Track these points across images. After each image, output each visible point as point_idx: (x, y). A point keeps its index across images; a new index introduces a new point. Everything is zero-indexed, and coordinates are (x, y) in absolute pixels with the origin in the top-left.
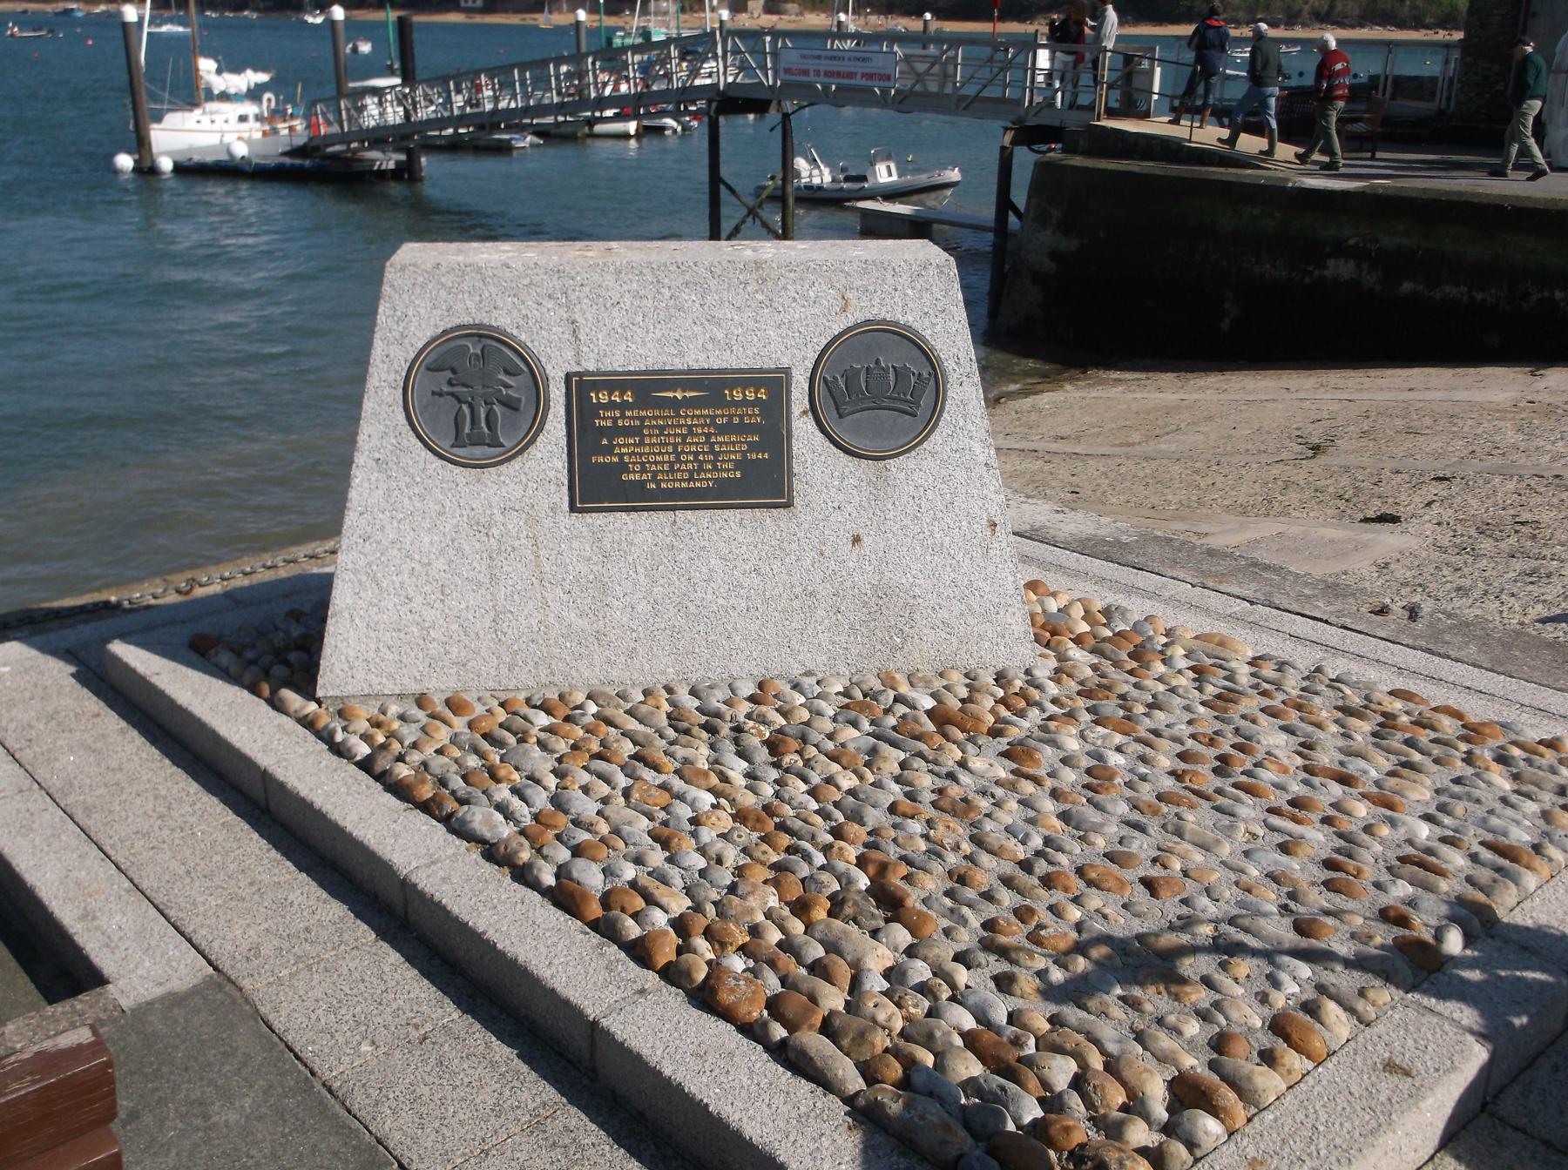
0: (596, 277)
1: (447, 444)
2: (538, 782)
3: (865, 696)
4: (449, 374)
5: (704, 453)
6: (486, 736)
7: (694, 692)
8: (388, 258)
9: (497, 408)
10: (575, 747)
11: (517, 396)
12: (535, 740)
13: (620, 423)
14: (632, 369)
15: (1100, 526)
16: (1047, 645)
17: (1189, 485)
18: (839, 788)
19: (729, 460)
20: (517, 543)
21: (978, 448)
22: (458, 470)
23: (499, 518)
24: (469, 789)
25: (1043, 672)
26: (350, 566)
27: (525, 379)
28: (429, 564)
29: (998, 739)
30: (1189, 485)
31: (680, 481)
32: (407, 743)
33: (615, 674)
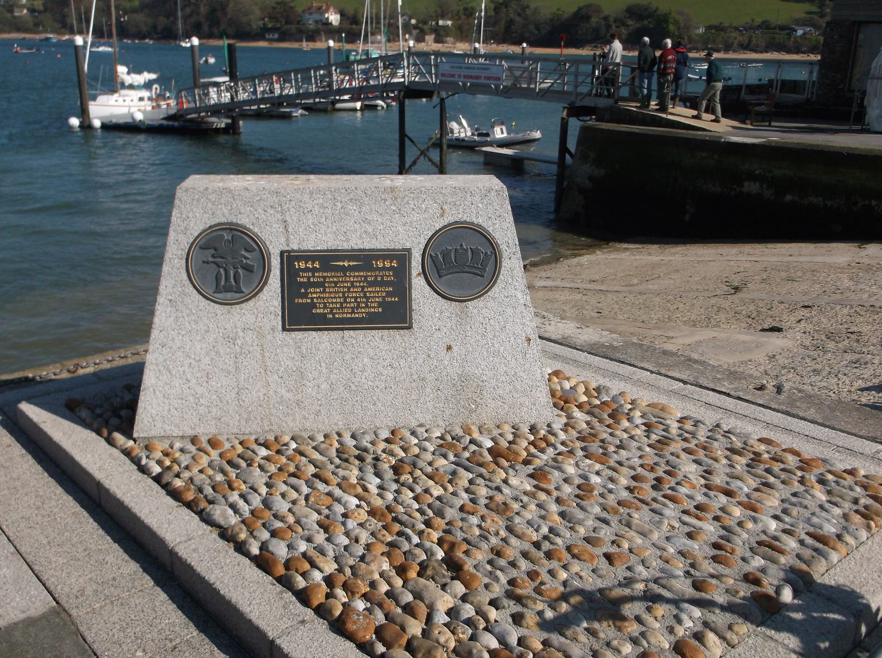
0: (298, 196)
1: (211, 293)
2: (256, 491)
3: (453, 439)
4: (212, 251)
5: (360, 297)
6: (230, 463)
7: (353, 436)
8: (179, 184)
9: (240, 271)
10: (280, 469)
11: (251, 263)
12: (257, 464)
13: (312, 280)
14: (319, 248)
15: (602, 336)
16: (562, 409)
17: (664, 309)
18: (432, 496)
19: (375, 302)
20: (251, 349)
21: (520, 295)
22: (217, 306)
23: (241, 334)
24: (215, 494)
25: (557, 426)
26: (154, 361)
27: (256, 253)
28: (200, 360)
29: (528, 466)
30: (664, 309)
31: (346, 313)
32: (183, 466)
33: (308, 425)
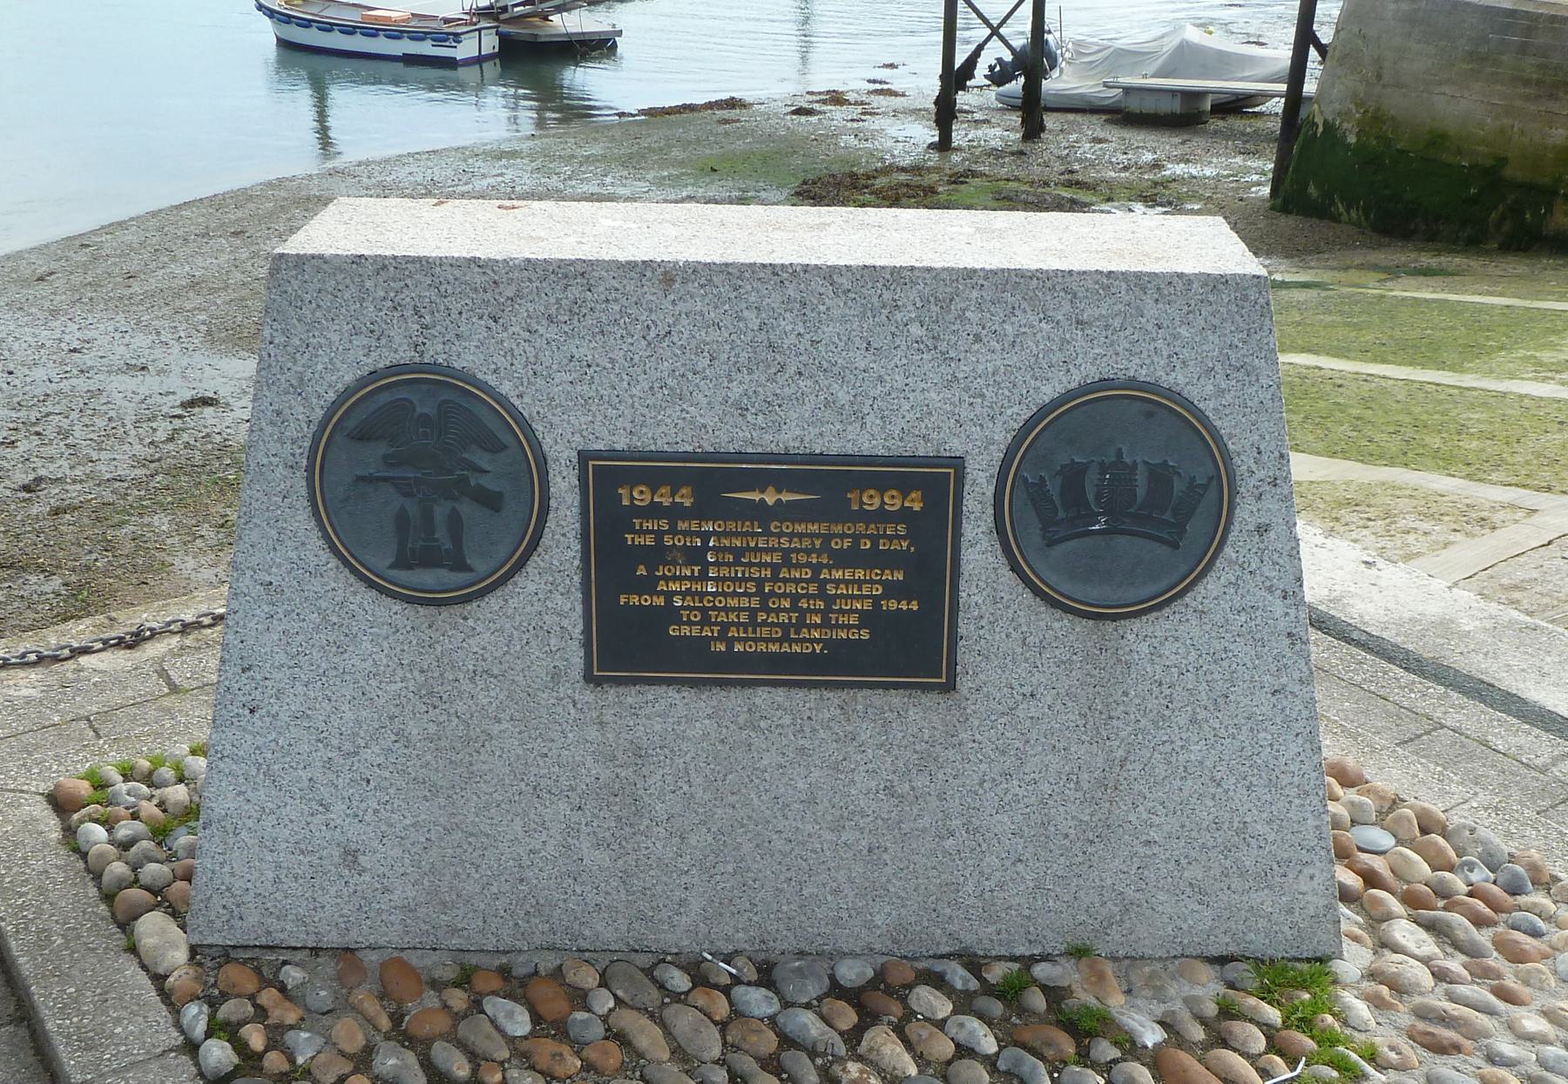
1: (383, 561)
5: (808, 596)
19: (851, 611)
20: (496, 729)
31: (767, 641)
